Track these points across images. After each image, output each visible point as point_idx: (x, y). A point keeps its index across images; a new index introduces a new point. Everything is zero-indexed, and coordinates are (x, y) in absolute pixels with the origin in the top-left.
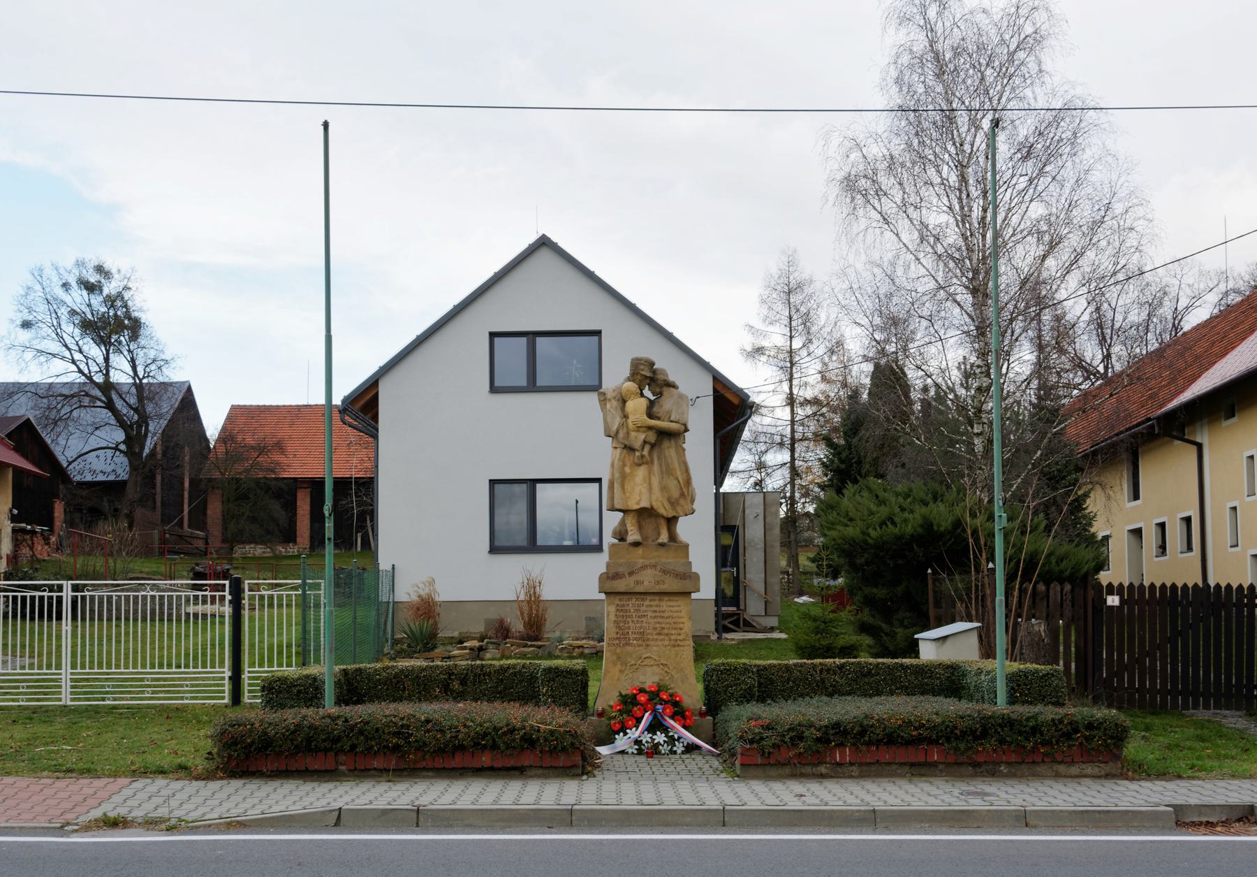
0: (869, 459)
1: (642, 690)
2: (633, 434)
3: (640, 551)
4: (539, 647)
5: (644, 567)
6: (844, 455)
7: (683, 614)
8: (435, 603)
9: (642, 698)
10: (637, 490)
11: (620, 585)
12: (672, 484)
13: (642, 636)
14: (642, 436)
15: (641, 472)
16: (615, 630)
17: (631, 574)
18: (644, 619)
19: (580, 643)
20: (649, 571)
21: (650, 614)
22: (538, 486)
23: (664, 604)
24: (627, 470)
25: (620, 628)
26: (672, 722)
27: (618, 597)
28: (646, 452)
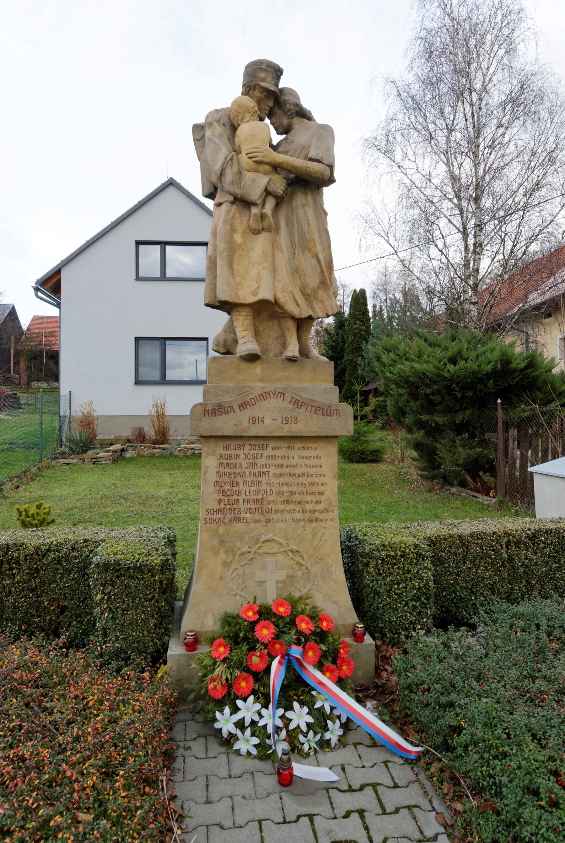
0: (350, 340)
1: (265, 613)
2: (248, 176)
3: (257, 369)
4: (164, 449)
5: (264, 396)
6: (334, 339)
7: (324, 469)
9: (265, 632)
10: (253, 272)
11: (225, 425)
13: (260, 505)
14: (263, 180)
15: (261, 243)
16: (216, 497)
17: (243, 406)
18: (264, 479)
20: (273, 402)
21: (272, 470)
22: (168, 342)
23: (294, 453)
24: (238, 238)
25: (224, 493)
26: (318, 674)
27: (221, 444)
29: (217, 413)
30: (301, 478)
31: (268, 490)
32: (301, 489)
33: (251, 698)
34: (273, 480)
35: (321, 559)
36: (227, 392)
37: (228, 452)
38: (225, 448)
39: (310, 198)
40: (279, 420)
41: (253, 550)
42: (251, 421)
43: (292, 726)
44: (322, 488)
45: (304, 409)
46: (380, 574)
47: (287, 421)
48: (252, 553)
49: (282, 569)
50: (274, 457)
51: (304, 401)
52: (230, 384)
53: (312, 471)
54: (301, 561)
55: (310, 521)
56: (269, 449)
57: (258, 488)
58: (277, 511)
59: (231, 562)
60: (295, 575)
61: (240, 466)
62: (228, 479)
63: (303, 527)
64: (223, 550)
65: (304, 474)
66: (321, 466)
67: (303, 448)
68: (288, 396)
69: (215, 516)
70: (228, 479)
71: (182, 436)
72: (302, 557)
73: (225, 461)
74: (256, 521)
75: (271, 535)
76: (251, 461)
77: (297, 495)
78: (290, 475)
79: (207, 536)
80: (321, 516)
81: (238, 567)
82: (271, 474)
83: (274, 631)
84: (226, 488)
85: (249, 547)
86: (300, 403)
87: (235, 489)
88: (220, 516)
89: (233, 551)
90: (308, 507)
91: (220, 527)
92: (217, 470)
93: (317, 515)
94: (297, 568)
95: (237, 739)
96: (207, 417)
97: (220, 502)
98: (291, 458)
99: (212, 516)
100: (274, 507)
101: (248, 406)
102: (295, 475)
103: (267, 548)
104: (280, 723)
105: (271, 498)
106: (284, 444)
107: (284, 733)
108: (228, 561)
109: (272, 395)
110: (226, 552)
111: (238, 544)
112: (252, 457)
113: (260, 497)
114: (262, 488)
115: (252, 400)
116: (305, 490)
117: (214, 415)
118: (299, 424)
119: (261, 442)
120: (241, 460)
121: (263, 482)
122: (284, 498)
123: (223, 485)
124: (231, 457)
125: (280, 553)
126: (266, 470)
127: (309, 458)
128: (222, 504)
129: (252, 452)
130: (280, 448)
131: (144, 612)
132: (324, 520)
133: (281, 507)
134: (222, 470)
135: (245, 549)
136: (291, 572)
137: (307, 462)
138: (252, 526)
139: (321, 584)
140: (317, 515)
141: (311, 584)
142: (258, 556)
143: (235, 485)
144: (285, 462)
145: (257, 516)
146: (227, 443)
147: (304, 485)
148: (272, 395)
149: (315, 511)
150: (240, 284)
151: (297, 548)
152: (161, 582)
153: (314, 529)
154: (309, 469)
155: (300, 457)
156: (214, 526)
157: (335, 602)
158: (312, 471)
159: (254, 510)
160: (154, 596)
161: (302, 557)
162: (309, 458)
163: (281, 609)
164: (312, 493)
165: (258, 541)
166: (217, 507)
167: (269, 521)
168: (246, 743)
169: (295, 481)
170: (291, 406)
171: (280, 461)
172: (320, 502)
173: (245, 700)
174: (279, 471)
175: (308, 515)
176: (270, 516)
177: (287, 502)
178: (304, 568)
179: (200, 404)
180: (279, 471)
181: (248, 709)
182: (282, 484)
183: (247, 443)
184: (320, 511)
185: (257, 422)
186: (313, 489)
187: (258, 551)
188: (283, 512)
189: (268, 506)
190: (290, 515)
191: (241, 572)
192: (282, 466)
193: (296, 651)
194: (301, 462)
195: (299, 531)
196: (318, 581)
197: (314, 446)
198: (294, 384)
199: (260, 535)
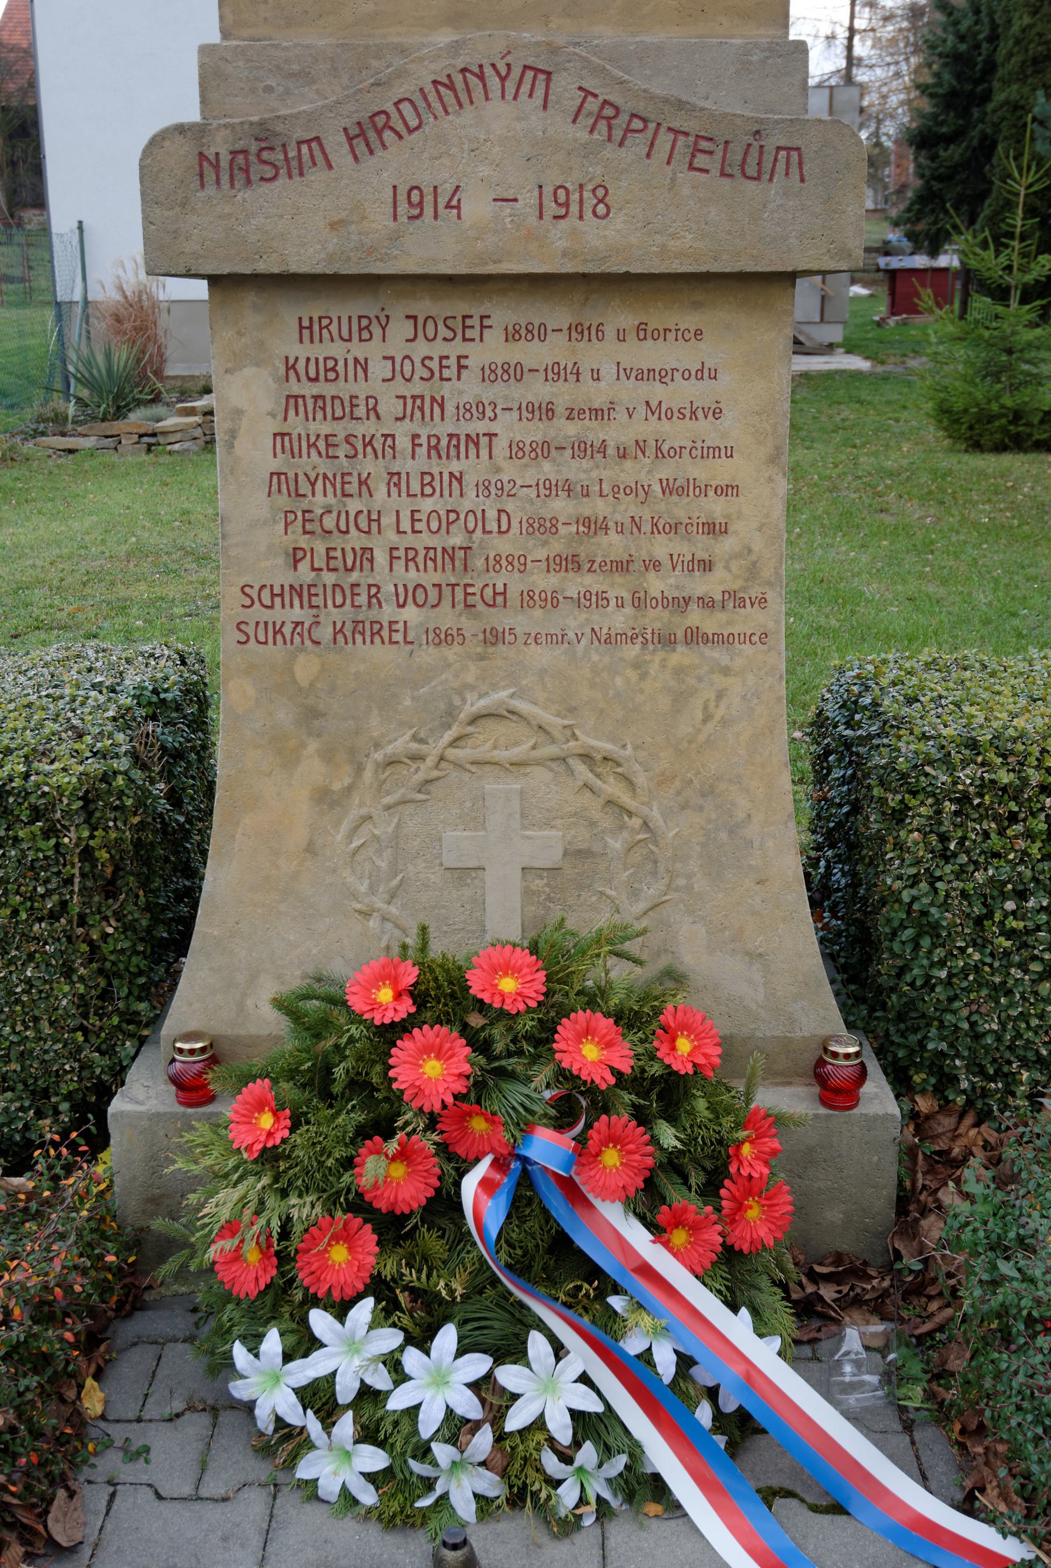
0: (1015, 28)
1: (441, 996)
5: (457, 87)
6: (964, 26)
7: (732, 428)
8: (155, 304)
9: (431, 1069)
11: (297, 224)
13: (457, 577)
17: (368, 134)
18: (472, 467)
20: (500, 117)
21: (509, 428)
23: (596, 355)
26: (638, 1237)
27: (291, 312)
29: (257, 170)
30: (628, 464)
31: (491, 514)
32: (628, 507)
33: (364, 1310)
34: (509, 471)
35: (708, 792)
36: (304, 76)
37: (319, 351)
38: (306, 330)
40: (528, 200)
42: (403, 208)
43: (515, 1421)
44: (717, 507)
45: (637, 144)
46: (947, 857)
47: (562, 204)
48: (430, 761)
49: (548, 824)
50: (514, 372)
51: (641, 108)
52: (318, 39)
53: (677, 433)
54: (625, 799)
55: (667, 641)
56: (494, 337)
57: (451, 503)
58: (528, 599)
59: (349, 790)
60: (597, 848)
61: (373, 411)
62: (324, 467)
63: (637, 665)
64: (313, 746)
65: (641, 446)
66: (717, 413)
67: (642, 332)
69: (277, 615)
70: (324, 467)
72: (628, 781)
73: (309, 390)
74: (443, 638)
75: (503, 694)
76: (418, 387)
77: (613, 536)
78: (582, 449)
79: (251, 691)
80: (711, 623)
81: (374, 812)
82: (501, 446)
83: (466, 1068)
84: (318, 501)
85: (415, 738)
86: (624, 118)
87: (353, 506)
88: (297, 613)
89: (352, 751)
90: (656, 585)
91: (301, 658)
92: (274, 426)
93: (695, 617)
94: (606, 822)
95: (311, 1446)
96: (211, 190)
98: (586, 376)
99: (267, 615)
100: (516, 584)
101: (388, 135)
102: (603, 448)
103: (485, 742)
104: (468, 1406)
105: (503, 546)
106: (558, 315)
107: (483, 1441)
108: (337, 786)
109: (494, 82)
110: (328, 755)
111: (375, 725)
112: (421, 372)
113: (457, 539)
114: (466, 504)
115: (406, 108)
116: (646, 514)
117: (240, 177)
119: (458, 306)
120: (375, 386)
121: (469, 479)
122: (557, 546)
123: (304, 488)
125: (539, 763)
126: (480, 427)
127: (663, 376)
128: (304, 566)
129: (421, 349)
130: (539, 333)
131: (31, 957)
134: (296, 424)
135: (401, 744)
136: (582, 837)
137: (657, 392)
138: (428, 656)
139: (700, 884)
140: (695, 617)
141: (661, 885)
142: (454, 775)
143: (353, 488)
144: (563, 394)
145: (447, 617)
146: (314, 309)
147: (640, 491)
148: (494, 82)
149: (687, 601)
151: (608, 747)
152: (87, 854)
153: (679, 672)
154: (666, 426)
155: (624, 372)
156: (275, 652)
157: (755, 957)
158: (677, 433)
159: (433, 594)
160: (64, 904)
161: (628, 781)
162: (663, 376)
163: (508, 985)
164: (675, 527)
165: (451, 713)
166: (283, 577)
167: (494, 637)
168: (344, 1463)
169: (605, 474)
171: (539, 390)
172: (707, 566)
173: (341, 1310)
174: (534, 432)
175: (656, 619)
176: (501, 619)
177: (571, 563)
178: (636, 822)
179: (181, 129)
180: (534, 432)
181: (351, 1346)
182: (550, 489)
183: (398, 310)
184: (707, 603)
185: (429, 210)
186: (680, 509)
187: (452, 753)
188: (552, 601)
189: (491, 578)
190: (583, 616)
191: (384, 828)
192: (548, 411)
193: (547, 1148)
194: (631, 392)
195: (619, 681)
196: (690, 876)
197: (689, 321)
199: (460, 692)
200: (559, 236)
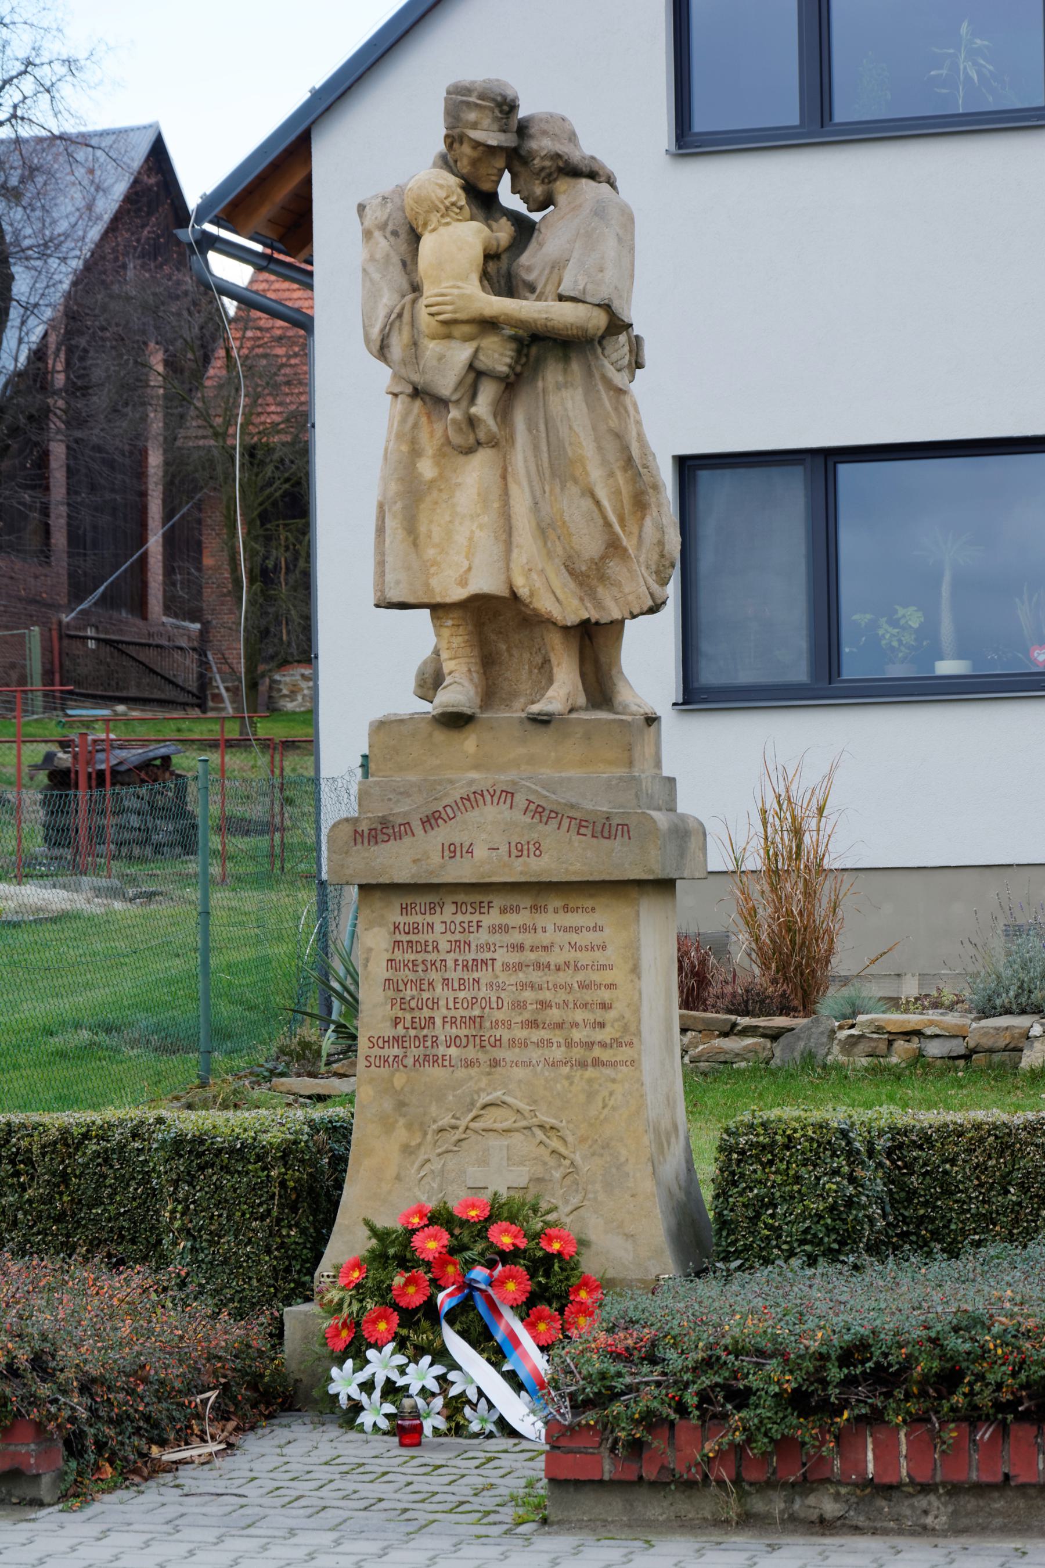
2: (432, 347)
3: (469, 742)
4: (774, 1035)
5: (472, 799)
9: (431, 1245)
10: (461, 538)
12: (574, 510)
13: (477, 1031)
14: (460, 354)
15: (475, 473)
17: (430, 821)
19: (912, 1020)
20: (491, 813)
21: (502, 956)
22: (846, 471)
24: (427, 469)
27: (396, 902)
28: (483, 407)
29: (380, 837)
30: (561, 974)
31: (494, 999)
32: (562, 995)
33: (390, 1347)
34: (502, 977)
35: (606, 1146)
36: (406, 794)
37: (411, 919)
38: (405, 910)
39: (575, 366)
40: (504, 849)
41: (463, 1123)
42: (447, 853)
43: (454, 1391)
44: (606, 995)
45: (553, 824)
46: (735, 1184)
48: (462, 1129)
49: (522, 1163)
50: (505, 929)
51: (554, 807)
52: (412, 777)
53: (584, 958)
54: (562, 1150)
55: (583, 1065)
57: (473, 994)
58: (512, 1043)
59: (419, 1145)
60: (547, 1177)
61: (436, 948)
62: (411, 976)
63: (568, 1077)
64: (402, 1122)
65: (567, 964)
66: (604, 948)
67: (566, 909)
68: (520, 799)
69: (386, 1052)
70: (411, 976)
71: (923, 977)
72: (562, 1139)
73: (405, 938)
74: (469, 1064)
75: (499, 1093)
76: (457, 936)
77: (555, 1010)
78: (538, 966)
79: (371, 1093)
80: (605, 1055)
81: (433, 1157)
82: (498, 965)
83: (446, 1242)
84: (408, 993)
85: (453, 1117)
86: (547, 812)
87: (425, 995)
88: (396, 1051)
89: (422, 1124)
90: (577, 1035)
91: (397, 1075)
92: (389, 956)
93: (597, 1052)
94: (552, 1162)
95: (362, 1409)
96: (359, 846)
97: (396, 1022)
98: (539, 930)
99: (381, 1052)
100: (506, 1035)
101: (440, 821)
102: (548, 966)
103: (492, 1119)
104: (433, 1386)
105: (500, 1015)
106: (526, 902)
107: (438, 1402)
108: (413, 1143)
109: (488, 798)
110: (409, 1127)
111: (433, 1110)
112: (459, 929)
113: (477, 1012)
114: (481, 994)
115: (448, 809)
116: (570, 998)
117: (373, 841)
118: (546, 857)
119: (478, 898)
120: (437, 936)
121: (483, 982)
122: (527, 1016)
123: (401, 987)
124: (416, 929)
125: (517, 1130)
126: (488, 955)
127: (577, 930)
128: (400, 1027)
129: (460, 917)
130: (517, 909)
131: (250, 1239)
132: (613, 1064)
133: (521, 1034)
134: (398, 955)
135: (446, 1120)
136: (539, 1171)
137: (574, 937)
138: (461, 1073)
139: (601, 1197)
140: (597, 1052)
141: (580, 1197)
142: (474, 1137)
143: (425, 987)
144: (528, 939)
145: (471, 1053)
147: (568, 988)
148: (488, 798)
149: (593, 1044)
150: (435, 563)
151: (553, 1121)
152: (283, 1184)
153: (590, 1081)
154: (579, 954)
155: (558, 928)
156: (384, 1071)
157: (628, 1236)
158: (584, 958)
159: (464, 1041)
160: (269, 1211)
161: (562, 1139)
162: (577, 930)
163: (473, 1213)
164: (585, 1005)
165: (473, 1104)
166: (389, 1032)
167: (495, 1063)
168: (375, 1413)
169: (550, 979)
170: (527, 819)
171: (517, 937)
172: (602, 1025)
174: (514, 958)
175: (577, 1053)
176: (499, 1054)
177: (534, 1024)
178: (567, 1162)
179: (347, 820)
180: (514, 958)
181: (382, 1363)
182: (523, 986)
183: (448, 900)
184: (603, 1045)
185: (458, 854)
186: (588, 996)
187: (473, 1125)
188: (524, 1044)
189: (493, 1032)
190: (540, 1052)
191: (436, 1165)
192: (521, 947)
193: (479, 1274)
195: (559, 1086)
196: (596, 1192)
197: (589, 903)
198: (547, 772)
199: (478, 1092)
200: (518, 865)
